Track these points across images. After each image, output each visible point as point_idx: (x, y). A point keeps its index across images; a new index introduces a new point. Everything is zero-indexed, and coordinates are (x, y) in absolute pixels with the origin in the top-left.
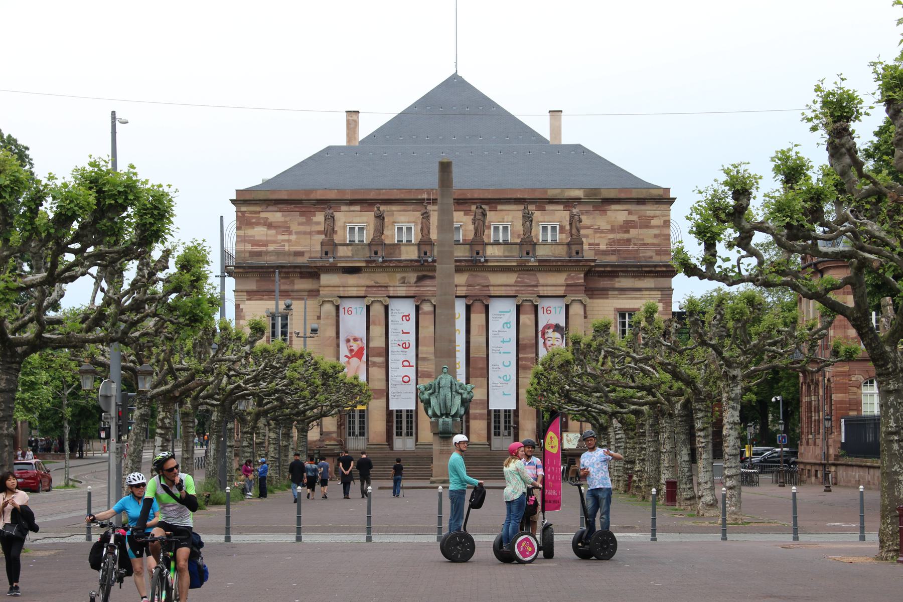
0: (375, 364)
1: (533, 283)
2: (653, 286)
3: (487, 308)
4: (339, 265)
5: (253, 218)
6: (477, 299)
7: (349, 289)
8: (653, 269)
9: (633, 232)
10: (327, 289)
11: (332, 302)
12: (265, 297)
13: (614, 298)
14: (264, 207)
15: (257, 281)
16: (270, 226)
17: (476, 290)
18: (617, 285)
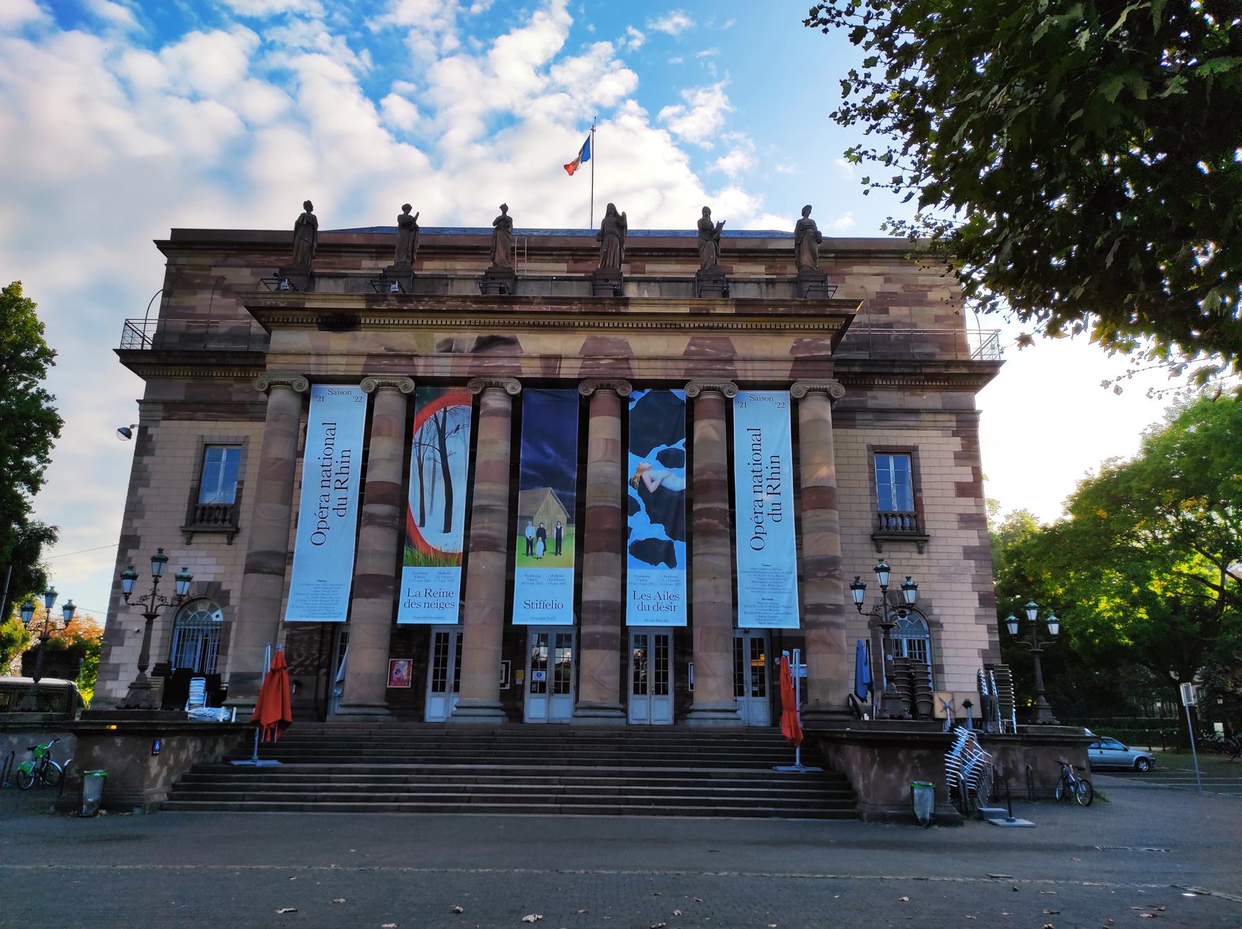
2: (939, 406)
4: (307, 305)
7: (330, 360)
8: (943, 370)
9: (896, 312)
10: (281, 359)
11: (288, 385)
12: (199, 415)
13: (865, 426)
16: (226, 290)
18: (871, 403)
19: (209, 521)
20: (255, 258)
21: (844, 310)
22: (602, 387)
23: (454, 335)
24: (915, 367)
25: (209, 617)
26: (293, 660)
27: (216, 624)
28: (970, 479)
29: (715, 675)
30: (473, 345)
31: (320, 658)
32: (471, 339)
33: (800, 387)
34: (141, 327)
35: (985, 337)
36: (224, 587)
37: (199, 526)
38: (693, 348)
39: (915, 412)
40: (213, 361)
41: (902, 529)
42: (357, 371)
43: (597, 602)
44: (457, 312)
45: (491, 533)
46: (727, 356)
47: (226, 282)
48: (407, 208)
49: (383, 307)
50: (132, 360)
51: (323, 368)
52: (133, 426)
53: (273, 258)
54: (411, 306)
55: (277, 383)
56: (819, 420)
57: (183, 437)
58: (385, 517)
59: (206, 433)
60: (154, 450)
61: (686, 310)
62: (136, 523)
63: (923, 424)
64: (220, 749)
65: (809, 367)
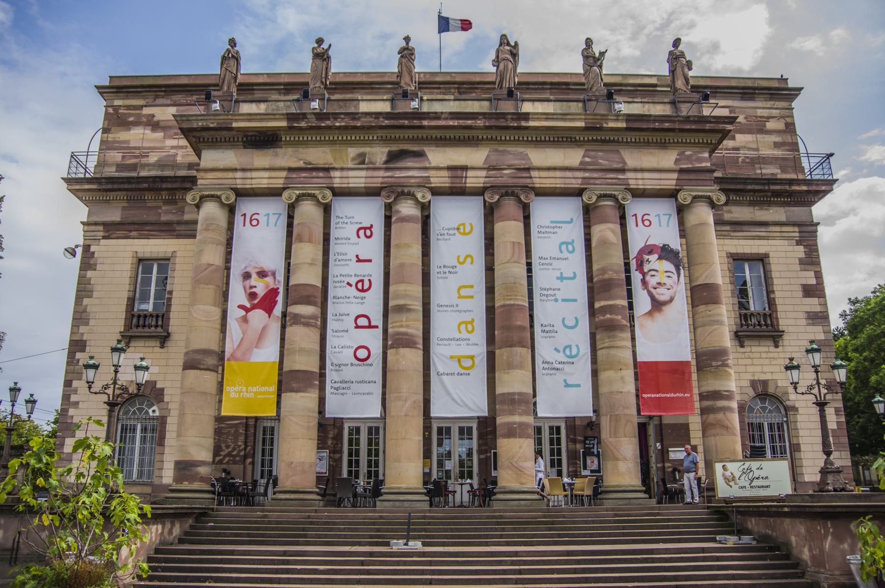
0: (297, 319)
1: (615, 166)
2: (783, 218)
3: (526, 209)
4: (235, 125)
5: (131, 115)
6: (508, 192)
7: (254, 174)
8: (787, 187)
10: (210, 175)
12: (133, 233)
14: (150, 101)
15: (124, 208)
16: (155, 126)
17: (506, 177)
19: (144, 326)
20: (178, 98)
21: (721, 126)
22: (507, 194)
23: (367, 150)
24: (764, 184)
25: (147, 412)
26: (222, 450)
27: (153, 418)
28: (813, 281)
29: (625, 459)
30: (384, 158)
31: (245, 449)
32: (382, 153)
33: (684, 197)
34: (83, 159)
35: (814, 161)
36: (159, 386)
37: (135, 331)
38: (587, 159)
39: (765, 224)
40: (145, 185)
41: (759, 327)
42: (279, 183)
43: (514, 394)
44: (370, 128)
45: (410, 331)
46: (620, 166)
47: (155, 119)
48: (320, 41)
49: (303, 124)
50: (78, 187)
51: (248, 181)
52: (77, 246)
53: (195, 97)
54: (328, 123)
55: (208, 196)
56: (704, 224)
57: (120, 255)
58: (310, 317)
59: (139, 249)
60: (96, 265)
61: (581, 124)
62: (82, 329)
63: (771, 234)
64: (177, 531)
65: (692, 176)
